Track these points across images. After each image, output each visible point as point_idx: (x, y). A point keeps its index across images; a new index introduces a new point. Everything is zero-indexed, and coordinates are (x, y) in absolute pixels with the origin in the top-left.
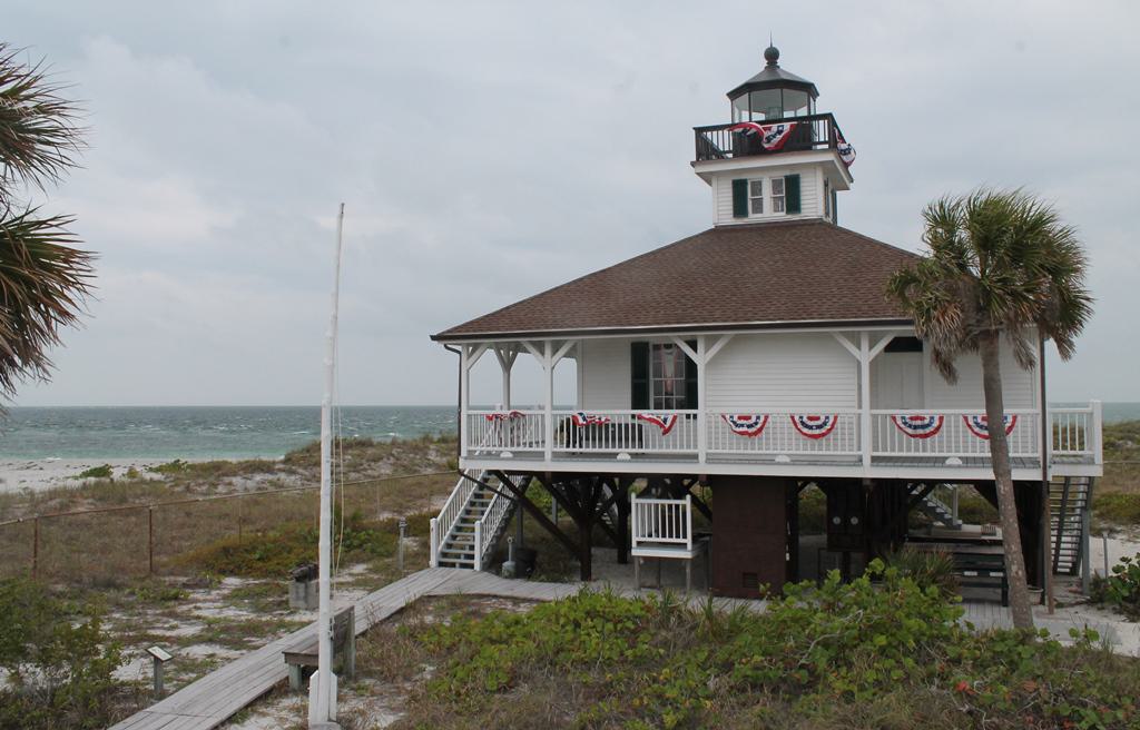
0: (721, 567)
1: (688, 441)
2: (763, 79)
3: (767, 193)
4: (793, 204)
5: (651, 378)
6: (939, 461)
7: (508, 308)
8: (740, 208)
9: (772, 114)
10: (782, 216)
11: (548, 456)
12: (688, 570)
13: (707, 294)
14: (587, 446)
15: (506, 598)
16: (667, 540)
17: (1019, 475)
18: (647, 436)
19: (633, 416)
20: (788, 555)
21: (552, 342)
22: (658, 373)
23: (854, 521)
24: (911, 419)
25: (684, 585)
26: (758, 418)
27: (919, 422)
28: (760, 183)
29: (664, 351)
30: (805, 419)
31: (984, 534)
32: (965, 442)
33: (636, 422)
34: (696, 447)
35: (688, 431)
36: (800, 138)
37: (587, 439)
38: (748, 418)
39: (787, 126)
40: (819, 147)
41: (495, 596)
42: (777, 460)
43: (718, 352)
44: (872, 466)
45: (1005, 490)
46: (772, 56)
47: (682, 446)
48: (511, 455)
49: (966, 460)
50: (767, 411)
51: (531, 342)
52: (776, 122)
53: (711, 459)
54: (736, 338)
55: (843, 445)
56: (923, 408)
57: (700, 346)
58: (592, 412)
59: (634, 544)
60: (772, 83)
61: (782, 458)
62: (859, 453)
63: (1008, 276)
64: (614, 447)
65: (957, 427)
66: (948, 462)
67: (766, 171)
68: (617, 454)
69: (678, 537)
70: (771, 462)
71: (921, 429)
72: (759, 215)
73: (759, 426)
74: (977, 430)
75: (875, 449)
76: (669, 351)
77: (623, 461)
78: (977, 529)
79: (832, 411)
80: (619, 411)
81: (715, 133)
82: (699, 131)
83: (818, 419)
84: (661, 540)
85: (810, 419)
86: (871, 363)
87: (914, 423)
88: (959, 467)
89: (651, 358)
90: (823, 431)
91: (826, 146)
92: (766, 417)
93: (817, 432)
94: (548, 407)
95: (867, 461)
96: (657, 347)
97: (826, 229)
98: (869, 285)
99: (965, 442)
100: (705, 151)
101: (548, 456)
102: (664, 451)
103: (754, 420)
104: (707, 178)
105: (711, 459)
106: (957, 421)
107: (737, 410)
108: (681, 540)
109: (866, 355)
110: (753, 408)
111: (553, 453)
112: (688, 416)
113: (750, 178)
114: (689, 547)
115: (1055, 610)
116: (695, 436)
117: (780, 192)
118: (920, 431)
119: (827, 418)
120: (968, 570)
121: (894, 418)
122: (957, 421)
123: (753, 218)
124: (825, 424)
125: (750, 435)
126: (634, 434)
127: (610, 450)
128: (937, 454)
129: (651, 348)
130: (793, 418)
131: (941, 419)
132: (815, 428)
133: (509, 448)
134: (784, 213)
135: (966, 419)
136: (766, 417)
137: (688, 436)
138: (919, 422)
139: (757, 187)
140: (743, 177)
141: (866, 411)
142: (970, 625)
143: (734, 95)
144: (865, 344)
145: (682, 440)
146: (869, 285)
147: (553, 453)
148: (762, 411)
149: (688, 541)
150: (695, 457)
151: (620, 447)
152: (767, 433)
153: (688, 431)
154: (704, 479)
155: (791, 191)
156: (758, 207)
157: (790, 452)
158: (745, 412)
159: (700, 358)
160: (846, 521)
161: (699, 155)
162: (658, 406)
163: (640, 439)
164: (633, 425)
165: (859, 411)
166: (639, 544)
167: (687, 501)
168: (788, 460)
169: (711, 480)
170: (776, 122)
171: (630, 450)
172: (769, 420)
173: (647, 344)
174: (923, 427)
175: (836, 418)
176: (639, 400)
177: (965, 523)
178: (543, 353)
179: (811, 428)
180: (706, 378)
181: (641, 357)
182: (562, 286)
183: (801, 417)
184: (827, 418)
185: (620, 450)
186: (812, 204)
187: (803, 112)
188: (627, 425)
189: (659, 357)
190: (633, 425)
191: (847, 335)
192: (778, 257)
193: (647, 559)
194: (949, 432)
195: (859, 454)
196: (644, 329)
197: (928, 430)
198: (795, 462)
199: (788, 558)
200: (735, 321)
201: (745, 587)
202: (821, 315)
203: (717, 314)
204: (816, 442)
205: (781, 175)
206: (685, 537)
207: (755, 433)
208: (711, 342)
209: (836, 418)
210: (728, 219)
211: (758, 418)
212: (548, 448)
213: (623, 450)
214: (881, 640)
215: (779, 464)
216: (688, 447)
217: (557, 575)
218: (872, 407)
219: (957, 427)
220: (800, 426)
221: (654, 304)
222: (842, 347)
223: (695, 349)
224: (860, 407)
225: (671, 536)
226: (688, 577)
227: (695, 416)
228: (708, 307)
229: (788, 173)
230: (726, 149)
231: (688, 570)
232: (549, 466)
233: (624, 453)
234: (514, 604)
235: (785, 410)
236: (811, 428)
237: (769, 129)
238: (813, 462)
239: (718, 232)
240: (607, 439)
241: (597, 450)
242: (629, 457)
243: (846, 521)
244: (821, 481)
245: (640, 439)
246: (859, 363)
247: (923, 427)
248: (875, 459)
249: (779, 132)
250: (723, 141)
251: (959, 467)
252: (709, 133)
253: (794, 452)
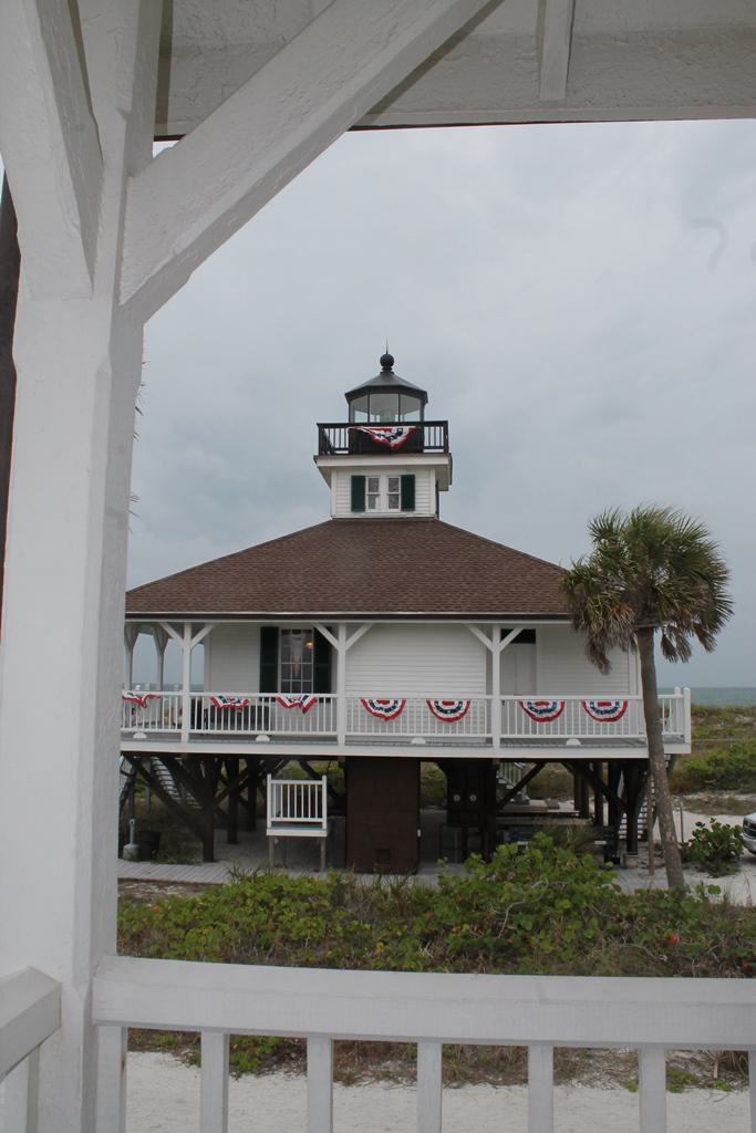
0: (342, 849)
1: (328, 723)
2: (380, 383)
4: (408, 501)
5: (280, 663)
6: (561, 743)
7: (141, 588)
8: (358, 502)
9: (385, 417)
10: (397, 512)
11: (185, 737)
12: (323, 849)
13: (342, 583)
14: (212, 728)
15: (148, 881)
16: (302, 819)
17: (669, 749)
18: (273, 718)
19: (261, 699)
20: (419, 832)
21: (193, 624)
22: (287, 657)
23: (473, 798)
24: (537, 704)
25: (319, 863)
26: (396, 702)
27: (545, 707)
28: (377, 481)
29: (292, 636)
30: (440, 704)
31: (550, 808)
32: (583, 725)
33: (263, 704)
34: (335, 729)
35: (328, 714)
36: (414, 445)
37: (212, 720)
38: (386, 702)
39: (406, 429)
40: (425, 451)
41: (136, 880)
42: (414, 742)
43: (361, 637)
44: (501, 747)
45: (660, 766)
46: (387, 362)
47: (294, 729)
48: (145, 737)
49: (583, 741)
50: (405, 695)
51: (172, 625)
52: (386, 425)
53: (350, 741)
54: (374, 629)
55: (475, 728)
56: (535, 694)
57: (342, 633)
58: (232, 695)
59: (269, 824)
60: (387, 386)
61: (418, 740)
62: (489, 735)
63: (652, 581)
64: (253, 729)
65: (576, 711)
66: (568, 743)
67: (383, 470)
68: (256, 736)
69: (313, 816)
70: (406, 743)
71: (542, 714)
72: (372, 510)
73: (397, 709)
74: (594, 713)
75: (504, 731)
76: (297, 636)
77: (263, 743)
78: (541, 803)
79: (464, 697)
80: (253, 695)
81: (332, 430)
82: (322, 426)
83: (452, 703)
84: (289, 819)
85: (445, 703)
86: (501, 653)
87: (539, 708)
88: (578, 747)
89: (280, 641)
90: (457, 715)
91: (442, 451)
92: (404, 702)
93: (452, 716)
94: (186, 686)
95: (496, 742)
96: (285, 632)
97: (433, 523)
98: (495, 582)
99: (583, 725)
100: (326, 448)
101: (185, 737)
102: (289, 733)
103: (392, 704)
104: (326, 473)
105: (350, 741)
106: (576, 706)
107: (374, 696)
108: (316, 820)
109: (497, 646)
110: (392, 693)
111: (191, 734)
112: (321, 700)
113: (368, 475)
114: (325, 826)
115: (656, 871)
116: (335, 718)
117: (396, 490)
118: (544, 715)
119: (461, 703)
120: (599, 839)
121: (521, 703)
122: (576, 706)
123: (369, 513)
124: (459, 708)
125: (387, 719)
126: (260, 717)
127: (249, 732)
128: (558, 736)
129: (280, 633)
130: (429, 702)
131: (563, 704)
132: (450, 712)
133: (143, 729)
134: (399, 510)
135: (584, 704)
136: (404, 702)
137: (328, 719)
138: (545, 707)
139: (375, 484)
140: (362, 474)
141: (496, 697)
142: (618, 888)
143: (351, 396)
144: (497, 635)
145: (321, 723)
146: (495, 582)
147: (191, 734)
148: (399, 696)
149: (324, 820)
150: (333, 739)
151: (259, 729)
152: (405, 717)
153: (328, 714)
154: (344, 760)
156: (372, 506)
157: (426, 735)
158: (384, 696)
159: (341, 644)
160: (465, 798)
161: (321, 449)
162: (285, 690)
163: (266, 722)
164: (260, 708)
165: (489, 697)
166: (275, 824)
167: (324, 782)
168: (423, 742)
169: (350, 762)
170: (386, 425)
171: (269, 732)
172: (407, 704)
173: (277, 629)
174: (550, 711)
175: (468, 703)
176: (267, 684)
177: (532, 798)
178: (183, 637)
179: (446, 712)
180: (347, 660)
181: (270, 640)
182: (194, 569)
183: (437, 702)
184: (461, 703)
185: (259, 732)
186: (424, 506)
187: (414, 417)
188: (253, 708)
189: (287, 642)
190: (260, 708)
191: (482, 628)
192: (402, 551)
193: (283, 839)
194: (569, 716)
195: (492, 733)
196: (284, 615)
197: (550, 715)
198: (430, 743)
199: (419, 832)
200: (377, 610)
201: (385, 859)
202: (458, 608)
203: (504, 608)
204: (450, 725)
205: (398, 474)
206: (320, 816)
207: (393, 717)
208: (351, 629)
209: (468, 703)
210: (345, 511)
211: (396, 702)
212: (186, 730)
213: (263, 732)
214: (566, 904)
215: (415, 745)
216: (328, 730)
217: (183, 858)
218: (502, 693)
219: (576, 711)
220: (435, 710)
221: (293, 591)
222: (479, 641)
223: (336, 636)
224: (489, 691)
225: (306, 816)
226: (323, 856)
227: (335, 699)
228: (348, 596)
229: (405, 473)
230: (337, 446)
231: (323, 849)
232: (186, 747)
233: (263, 735)
234: (160, 887)
235: (423, 695)
236: (446, 712)
237: (390, 430)
238: (446, 744)
239: (336, 523)
240: (233, 721)
241: (215, 731)
242: (268, 739)
243: (465, 798)
244: (440, 762)
245: (266, 722)
246: (489, 654)
247: (550, 711)
248: (503, 741)
249: (399, 434)
250: (340, 439)
251: (578, 747)
252: (326, 430)
253: (429, 734)
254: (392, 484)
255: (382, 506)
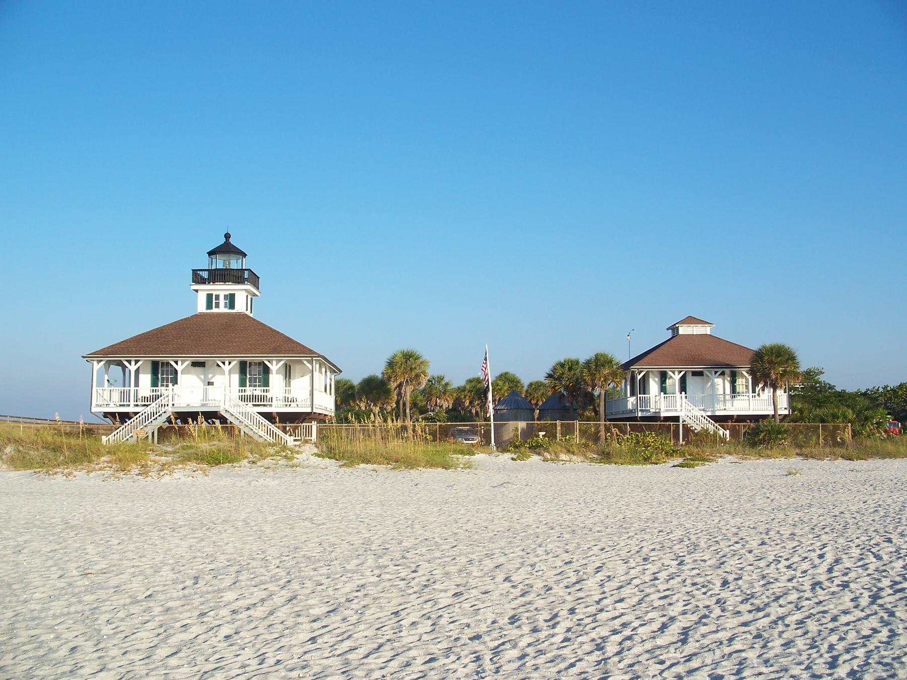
3: (222, 301)
4: (232, 306)
8: (209, 306)
10: (227, 311)
46: (227, 236)
60: (227, 249)
123: (215, 310)
139: (217, 297)
143: (210, 253)
155: (231, 299)
156: (217, 306)
186: (240, 306)
205: (227, 293)
254: (226, 296)
255: (223, 309)
